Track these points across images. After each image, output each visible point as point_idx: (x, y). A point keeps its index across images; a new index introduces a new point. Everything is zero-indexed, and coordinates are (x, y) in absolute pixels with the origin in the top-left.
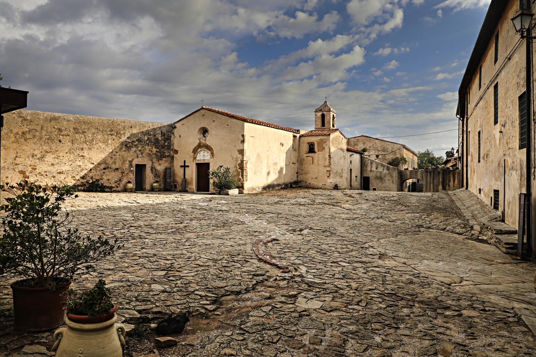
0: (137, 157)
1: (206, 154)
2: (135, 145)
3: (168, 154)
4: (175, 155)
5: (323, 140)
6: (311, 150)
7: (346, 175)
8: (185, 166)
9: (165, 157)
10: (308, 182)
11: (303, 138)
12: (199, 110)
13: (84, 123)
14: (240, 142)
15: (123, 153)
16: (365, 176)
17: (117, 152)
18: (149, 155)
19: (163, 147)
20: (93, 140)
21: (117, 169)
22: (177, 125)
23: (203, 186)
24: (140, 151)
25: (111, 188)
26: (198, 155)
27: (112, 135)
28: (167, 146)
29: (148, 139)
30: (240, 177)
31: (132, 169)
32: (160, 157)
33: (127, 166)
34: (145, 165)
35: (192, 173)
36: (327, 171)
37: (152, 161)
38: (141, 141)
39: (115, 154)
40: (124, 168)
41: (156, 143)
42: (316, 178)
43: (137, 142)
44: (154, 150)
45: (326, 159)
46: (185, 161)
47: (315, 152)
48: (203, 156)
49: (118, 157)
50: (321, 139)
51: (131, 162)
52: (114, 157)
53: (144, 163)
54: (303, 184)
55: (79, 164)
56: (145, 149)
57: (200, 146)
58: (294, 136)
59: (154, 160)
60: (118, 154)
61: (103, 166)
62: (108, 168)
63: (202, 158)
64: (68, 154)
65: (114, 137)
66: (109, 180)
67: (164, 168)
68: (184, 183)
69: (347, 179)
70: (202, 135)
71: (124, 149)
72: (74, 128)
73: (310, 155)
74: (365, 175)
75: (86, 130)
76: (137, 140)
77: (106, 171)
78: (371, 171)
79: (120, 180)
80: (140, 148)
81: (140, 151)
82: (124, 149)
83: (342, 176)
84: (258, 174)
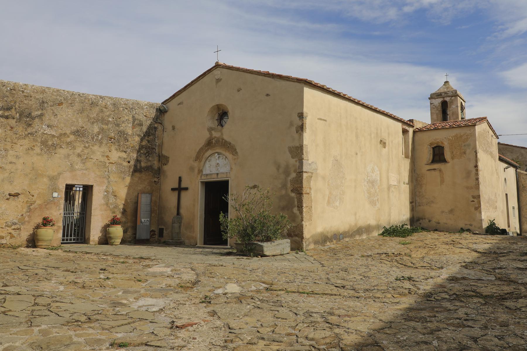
1: (221, 161)
2: (68, 144)
5: (461, 137)
6: (438, 155)
8: (180, 190)
10: (434, 220)
11: (419, 135)
17: (17, 157)
22: (171, 105)
23: (214, 235)
24: (79, 155)
26: (207, 165)
29: (102, 130)
30: (295, 210)
31: (55, 195)
34: (92, 186)
35: (194, 204)
36: (474, 197)
38: (83, 135)
39: (14, 160)
40: (35, 193)
43: (72, 137)
45: (468, 173)
46: (180, 178)
47: (444, 161)
48: (216, 167)
53: (90, 184)
56: (93, 152)
57: (209, 144)
58: (405, 132)
60: (21, 161)
63: (214, 171)
65: (12, 122)
70: (216, 123)
71: (37, 150)
81: (79, 155)
82: (37, 150)
83: (496, 208)
84: (337, 204)
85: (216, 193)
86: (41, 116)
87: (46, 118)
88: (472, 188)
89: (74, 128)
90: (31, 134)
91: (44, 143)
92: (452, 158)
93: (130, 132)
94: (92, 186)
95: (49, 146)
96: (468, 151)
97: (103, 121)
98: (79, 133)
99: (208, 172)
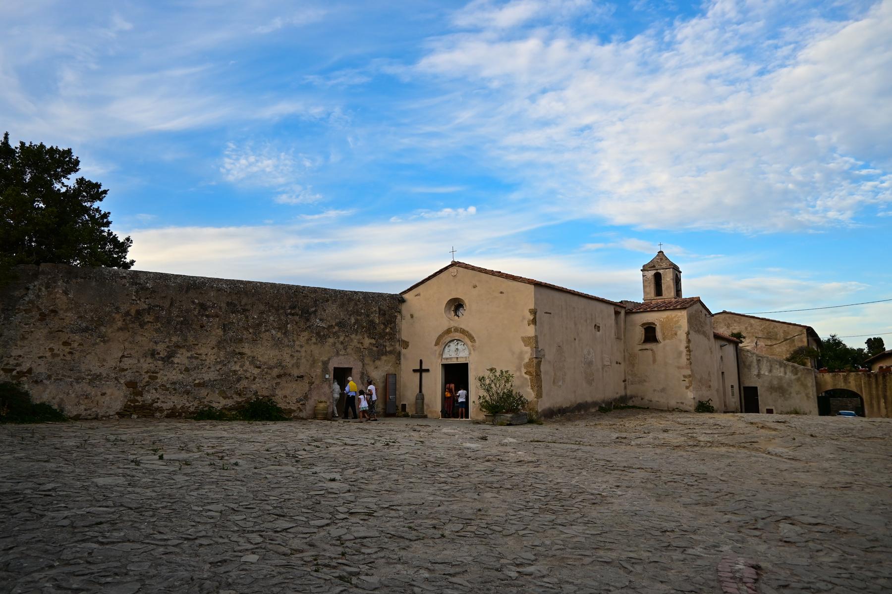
0: (338, 354)
3: (391, 348)
4: (403, 351)
7: (715, 383)
8: (421, 371)
9: (385, 353)
10: (646, 398)
12: (446, 268)
13: (246, 293)
14: (526, 322)
15: (313, 347)
16: (747, 385)
18: (358, 350)
19: (382, 336)
20: (260, 325)
21: (302, 377)
24: (342, 343)
25: (291, 411)
27: (293, 315)
28: (390, 334)
29: (357, 320)
31: (327, 376)
32: (379, 353)
33: (319, 371)
34: (351, 369)
36: (685, 376)
37: (362, 361)
39: (299, 349)
40: (313, 375)
41: (369, 329)
42: (663, 390)
44: (367, 341)
45: (680, 353)
46: (421, 361)
48: (456, 353)
49: (303, 354)
50: (667, 317)
51: (325, 364)
52: (296, 354)
54: (637, 402)
55: (233, 368)
56: (352, 340)
57: (448, 331)
59: (367, 360)
60: (304, 349)
61: (276, 372)
62: (285, 374)
63: (453, 355)
64: (215, 350)
65: (297, 318)
66: (285, 397)
67: (384, 374)
68: (419, 401)
69: (717, 391)
71: (314, 340)
72: (228, 304)
73: (648, 346)
74: (751, 382)
75: (249, 307)
76: (337, 324)
77: (283, 381)
78: (759, 375)
79: (306, 397)
80: (341, 339)
81: (342, 343)
82: (314, 340)
85: (456, 374)
86: (316, 311)
87: (319, 313)
88: (683, 368)
89: (338, 320)
90: (309, 327)
91: (318, 334)
92: (664, 339)
93: (377, 321)
94: (351, 369)
95: (321, 337)
96: (679, 333)
97: (358, 313)
98: (341, 324)
99: (448, 356)
